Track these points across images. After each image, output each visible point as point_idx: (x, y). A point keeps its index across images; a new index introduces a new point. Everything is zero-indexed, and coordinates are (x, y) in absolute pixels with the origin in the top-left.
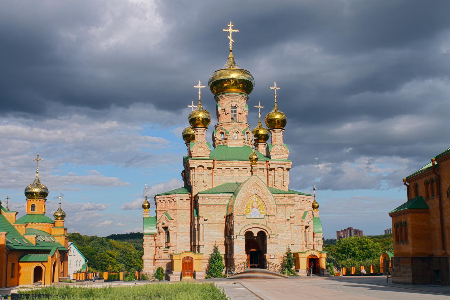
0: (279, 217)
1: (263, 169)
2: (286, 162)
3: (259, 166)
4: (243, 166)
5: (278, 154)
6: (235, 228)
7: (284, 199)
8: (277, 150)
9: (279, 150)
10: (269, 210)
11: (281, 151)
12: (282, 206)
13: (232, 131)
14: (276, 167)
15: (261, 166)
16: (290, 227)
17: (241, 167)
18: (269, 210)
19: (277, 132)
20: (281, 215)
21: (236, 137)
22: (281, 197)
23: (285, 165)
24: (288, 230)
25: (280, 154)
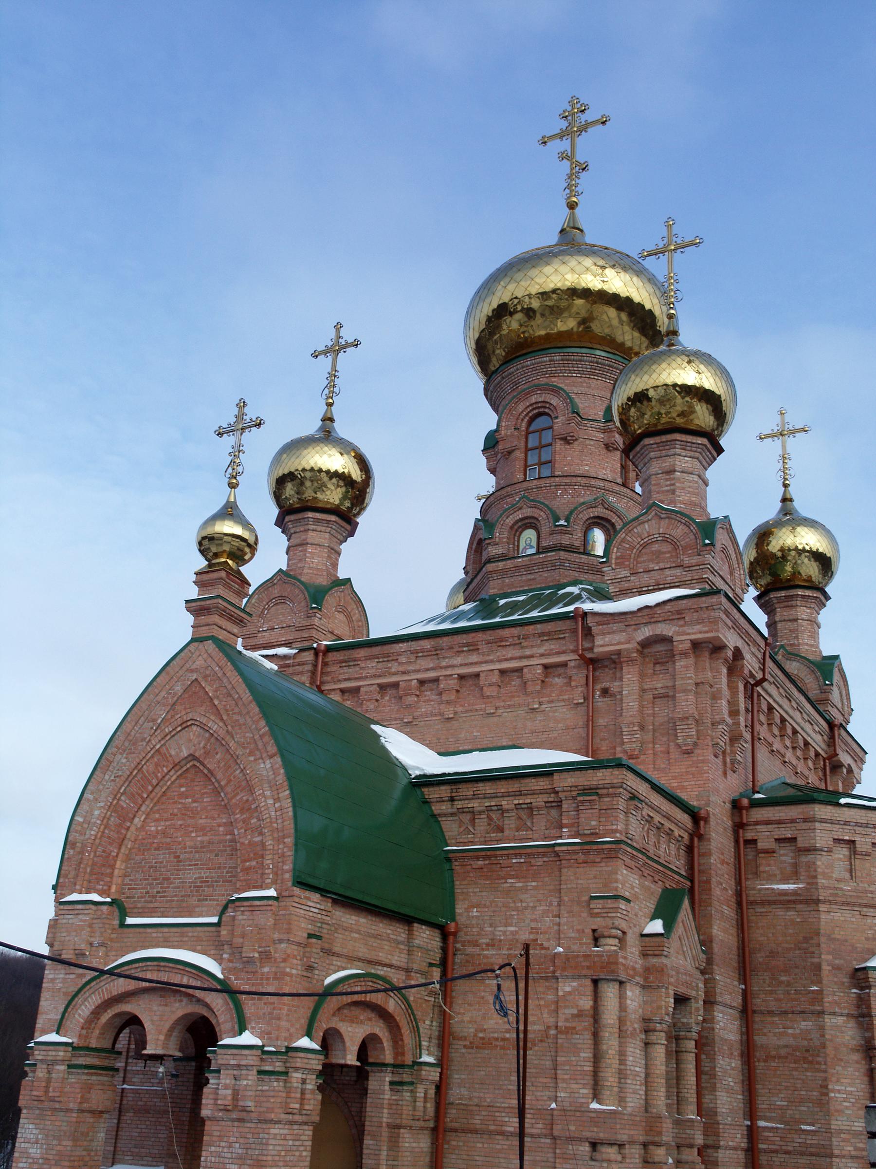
0: (517, 932)
1: (564, 665)
2: (685, 602)
3: (541, 650)
4: (458, 660)
5: (652, 566)
6: (48, 990)
7: (554, 813)
8: (645, 546)
9: (655, 547)
10: (254, 863)
11: (669, 547)
12: (539, 861)
13: (510, 521)
14: (629, 642)
15: (553, 646)
16: (586, 1003)
17: (448, 672)
18: (254, 863)
19: (658, 454)
20: (532, 921)
21: (532, 547)
22: (539, 801)
23: (681, 622)
24: (569, 1031)
25: (662, 565)
